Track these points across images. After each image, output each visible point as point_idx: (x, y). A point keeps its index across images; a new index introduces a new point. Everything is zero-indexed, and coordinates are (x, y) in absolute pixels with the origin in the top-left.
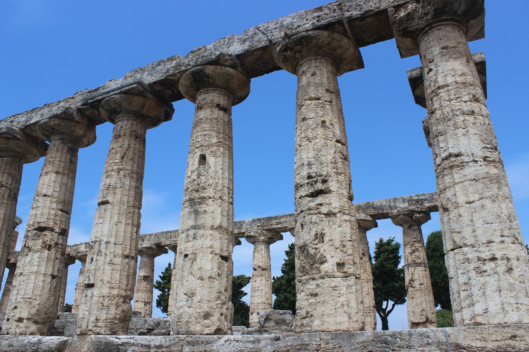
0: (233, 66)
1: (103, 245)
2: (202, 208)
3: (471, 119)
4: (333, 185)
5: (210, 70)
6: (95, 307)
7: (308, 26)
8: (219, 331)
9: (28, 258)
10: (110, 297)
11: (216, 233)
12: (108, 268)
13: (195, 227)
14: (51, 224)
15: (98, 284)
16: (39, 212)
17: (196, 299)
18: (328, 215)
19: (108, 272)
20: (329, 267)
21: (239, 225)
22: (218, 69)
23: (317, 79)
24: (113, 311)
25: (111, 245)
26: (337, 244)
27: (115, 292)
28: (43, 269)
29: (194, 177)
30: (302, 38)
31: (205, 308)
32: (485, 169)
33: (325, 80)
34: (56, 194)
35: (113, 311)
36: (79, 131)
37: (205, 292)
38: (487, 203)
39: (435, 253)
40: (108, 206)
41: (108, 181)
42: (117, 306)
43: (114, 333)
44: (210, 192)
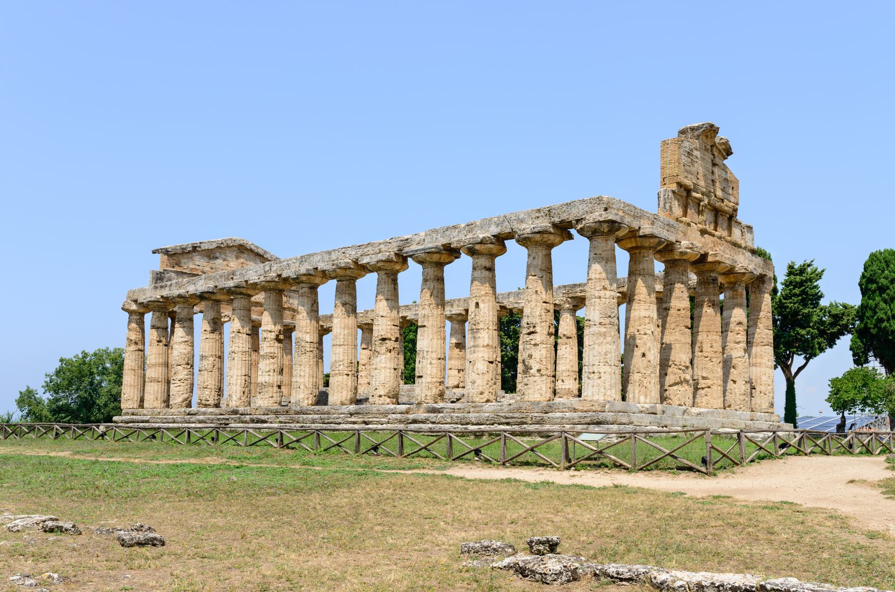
2: (478, 335)
4: (538, 329)
5: (477, 247)
7: (528, 231)
8: (488, 401)
9: (378, 359)
11: (485, 349)
12: (429, 366)
13: (474, 346)
14: (389, 336)
15: (425, 376)
16: (380, 328)
18: (535, 345)
19: (429, 369)
23: (535, 262)
27: (434, 380)
28: (388, 365)
30: (525, 239)
31: (481, 389)
33: (540, 262)
36: (397, 267)
38: (596, 346)
39: (870, 286)
41: (423, 312)
42: (436, 388)
44: (481, 326)
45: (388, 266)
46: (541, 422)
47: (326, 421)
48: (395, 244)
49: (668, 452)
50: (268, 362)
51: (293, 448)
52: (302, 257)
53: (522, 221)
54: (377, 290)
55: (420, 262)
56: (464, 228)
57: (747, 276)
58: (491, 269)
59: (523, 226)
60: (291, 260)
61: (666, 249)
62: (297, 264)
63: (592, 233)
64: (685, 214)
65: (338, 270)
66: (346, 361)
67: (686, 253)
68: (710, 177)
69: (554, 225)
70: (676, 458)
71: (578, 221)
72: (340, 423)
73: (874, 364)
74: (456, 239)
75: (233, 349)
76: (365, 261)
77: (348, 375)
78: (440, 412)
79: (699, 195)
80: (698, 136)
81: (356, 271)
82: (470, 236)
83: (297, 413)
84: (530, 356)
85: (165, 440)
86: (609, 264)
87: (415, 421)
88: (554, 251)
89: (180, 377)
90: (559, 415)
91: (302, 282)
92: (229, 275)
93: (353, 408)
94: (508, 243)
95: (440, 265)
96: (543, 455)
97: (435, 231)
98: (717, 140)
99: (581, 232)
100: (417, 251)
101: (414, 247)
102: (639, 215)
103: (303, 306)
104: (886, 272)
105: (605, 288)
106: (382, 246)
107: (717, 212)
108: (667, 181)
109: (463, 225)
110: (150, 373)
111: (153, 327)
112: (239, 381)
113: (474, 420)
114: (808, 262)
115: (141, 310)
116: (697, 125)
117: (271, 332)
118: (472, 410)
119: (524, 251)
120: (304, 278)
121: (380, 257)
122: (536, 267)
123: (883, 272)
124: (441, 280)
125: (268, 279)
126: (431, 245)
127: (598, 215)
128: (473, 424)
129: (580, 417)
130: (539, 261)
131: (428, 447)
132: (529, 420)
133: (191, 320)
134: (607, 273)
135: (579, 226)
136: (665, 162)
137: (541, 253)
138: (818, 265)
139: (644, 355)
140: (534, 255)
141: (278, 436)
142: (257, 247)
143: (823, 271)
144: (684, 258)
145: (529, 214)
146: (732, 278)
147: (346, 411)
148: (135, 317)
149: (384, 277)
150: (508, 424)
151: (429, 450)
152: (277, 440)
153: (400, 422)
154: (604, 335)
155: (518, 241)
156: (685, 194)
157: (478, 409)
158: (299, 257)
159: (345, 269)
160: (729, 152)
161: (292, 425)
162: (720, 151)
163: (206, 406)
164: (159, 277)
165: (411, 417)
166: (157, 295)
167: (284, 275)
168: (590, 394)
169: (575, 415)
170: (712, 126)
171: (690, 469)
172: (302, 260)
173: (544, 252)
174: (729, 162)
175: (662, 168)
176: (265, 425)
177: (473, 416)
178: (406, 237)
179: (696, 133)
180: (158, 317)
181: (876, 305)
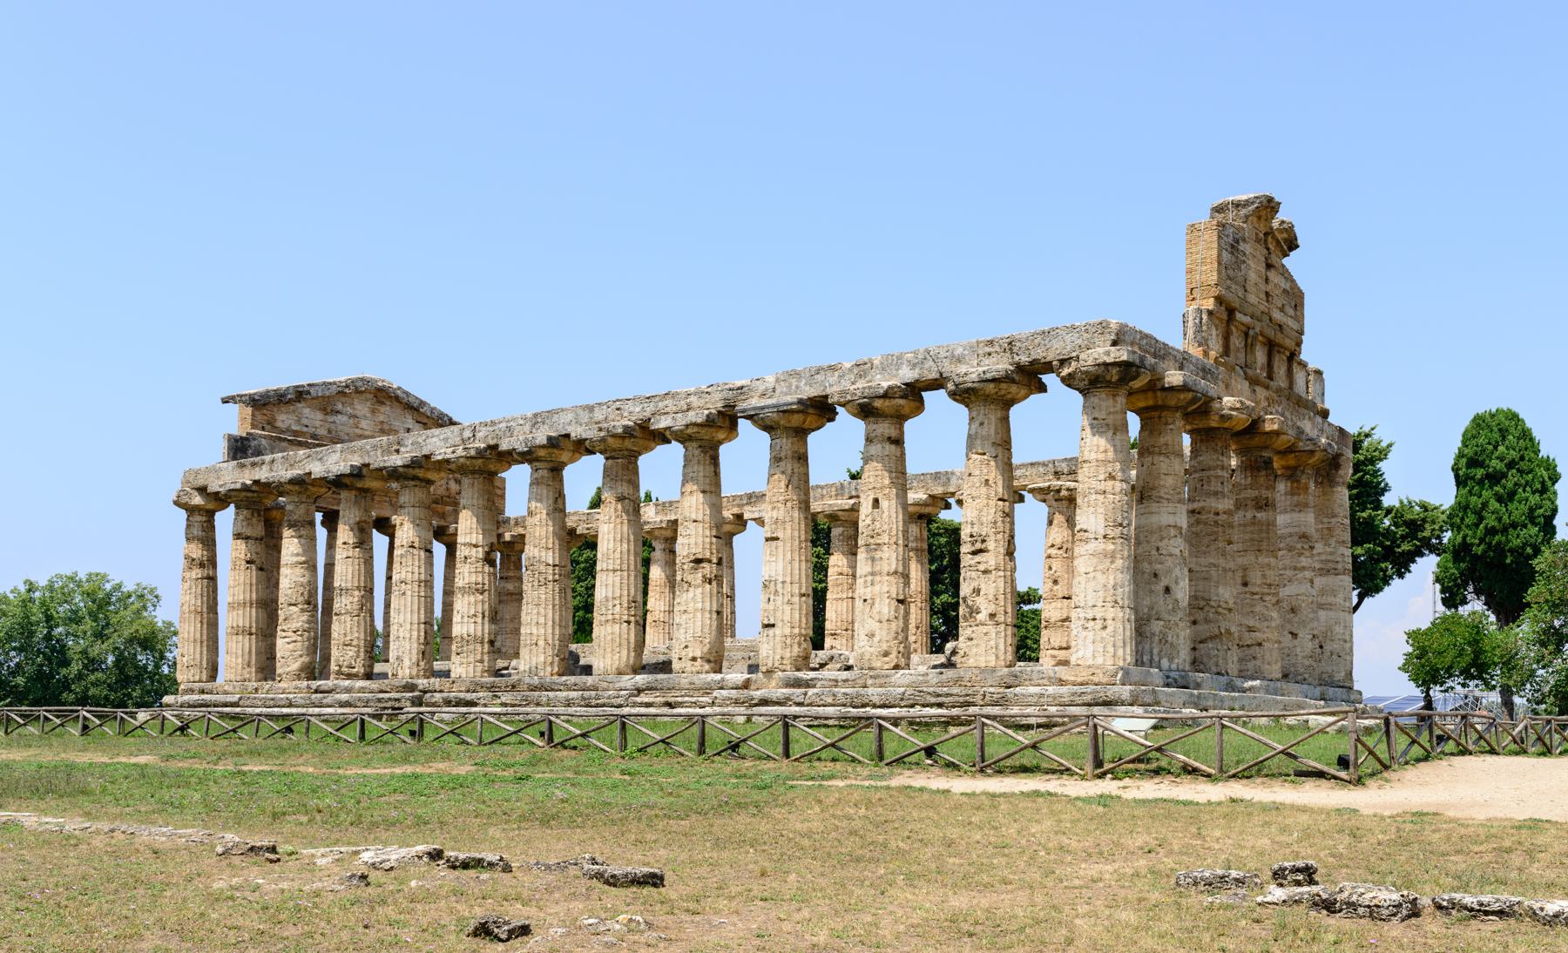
0: (903, 397)
1: (779, 586)
2: (878, 555)
3: (1101, 497)
4: (991, 545)
5: (878, 403)
6: (779, 647)
7: (974, 377)
9: (691, 594)
10: (792, 636)
11: (891, 578)
12: (787, 608)
13: (873, 574)
14: (708, 555)
15: (779, 624)
17: (876, 639)
18: (985, 572)
19: (788, 612)
20: (982, 617)
21: (944, 479)
22: (887, 403)
24: (796, 649)
25: (788, 586)
26: (991, 597)
27: (796, 631)
29: (868, 521)
30: (968, 391)
31: (885, 647)
32: (1102, 546)
34: (707, 518)
35: (796, 649)
37: (884, 633)
38: (1099, 575)
40: (780, 543)
42: (800, 644)
43: (798, 670)
45: (706, 434)
46: (1001, 702)
47: (594, 702)
48: (718, 396)
49: (1281, 748)
50: (472, 599)
51: (575, 748)
52: (536, 415)
53: (960, 360)
54: (684, 475)
55: (768, 428)
56: (850, 370)
57: (1318, 456)
58: (898, 441)
59: (963, 369)
60: (514, 419)
61: (1196, 410)
62: (527, 428)
63: (1091, 383)
64: (1226, 351)
65: (610, 440)
66: (625, 599)
67: (1230, 417)
68: (1263, 287)
69: (1020, 368)
70: (1295, 757)
71: (1063, 362)
72: (620, 706)
73: (1475, 606)
74: (833, 387)
75: (403, 575)
76: (662, 423)
77: (629, 622)
78: (808, 686)
79: (1246, 320)
80: (1247, 217)
81: (641, 442)
82: (861, 384)
83: (533, 688)
84: (977, 591)
85: (313, 736)
86: (1118, 437)
87: (764, 702)
88: (1016, 412)
89: (295, 625)
90: (1032, 690)
91: (537, 460)
92: (390, 444)
93: (641, 679)
94: (927, 396)
95: (802, 433)
96: (1052, 752)
97: (795, 374)
98: (1275, 224)
99: (1068, 381)
100: (763, 408)
101: (755, 402)
102: (1163, 352)
103: (540, 501)
104: (1501, 448)
105: (1112, 477)
106: (693, 399)
107: (1272, 347)
108: (1196, 293)
109: (848, 365)
110: (227, 619)
111: (238, 536)
112: (415, 634)
113: (876, 700)
114: (1366, 429)
115: (210, 506)
116: (1244, 197)
117: (476, 546)
118: (870, 682)
119: (961, 411)
120: (542, 453)
121: (692, 417)
122: (984, 438)
123: (1496, 448)
124: (802, 458)
125: (473, 453)
126: (789, 399)
127: (1102, 352)
128: (875, 706)
129: (1074, 694)
130: (991, 429)
131: (840, 744)
132: (978, 699)
133: (312, 524)
134: (1115, 451)
135: (1065, 372)
136: (1194, 262)
137: (994, 416)
138: (1382, 436)
139: (1167, 590)
140: (981, 418)
141: (544, 727)
142: (407, 394)
143: (1390, 445)
144: (1226, 425)
145: (973, 348)
146: (1291, 460)
147: (629, 685)
148: (198, 518)
149: (697, 452)
150: (940, 705)
151: (840, 749)
152: (542, 734)
153: (737, 702)
154: (1112, 557)
155: (953, 395)
156: (1225, 317)
157: (882, 681)
158: (529, 415)
159: (621, 437)
160: (1292, 244)
161: (528, 709)
162: (1278, 242)
163: (350, 676)
164: (240, 448)
165: (758, 694)
166: (247, 477)
167: (504, 447)
168: (1089, 654)
169: (1064, 690)
170: (1270, 200)
171: (1320, 775)
172: (536, 420)
173: (999, 414)
174: (1291, 262)
175: (1189, 271)
176: (474, 709)
177: (874, 693)
178: (739, 383)
179: (1243, 212)
180: (247, 519)
181: (1485, 505)
